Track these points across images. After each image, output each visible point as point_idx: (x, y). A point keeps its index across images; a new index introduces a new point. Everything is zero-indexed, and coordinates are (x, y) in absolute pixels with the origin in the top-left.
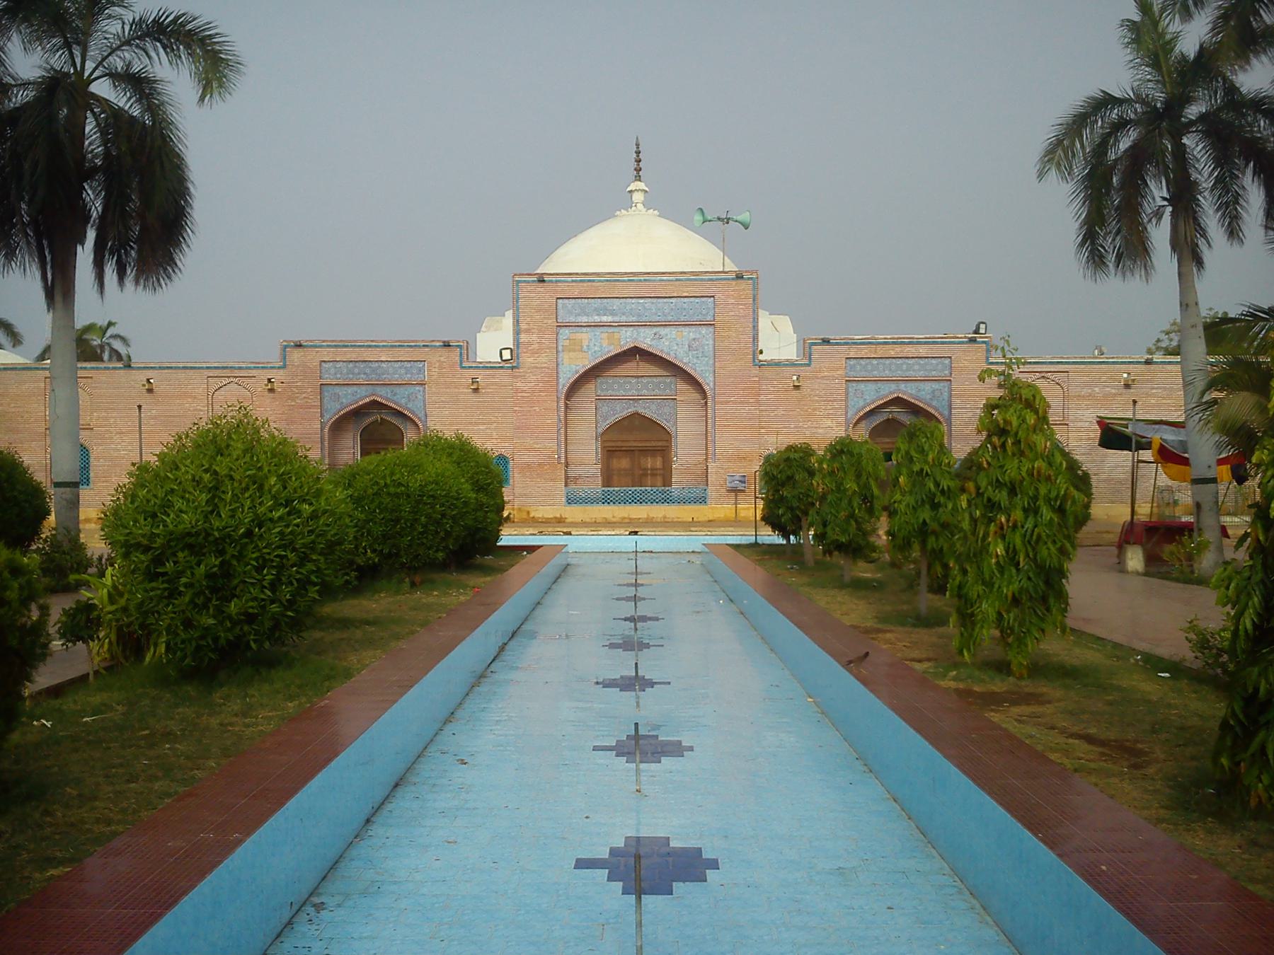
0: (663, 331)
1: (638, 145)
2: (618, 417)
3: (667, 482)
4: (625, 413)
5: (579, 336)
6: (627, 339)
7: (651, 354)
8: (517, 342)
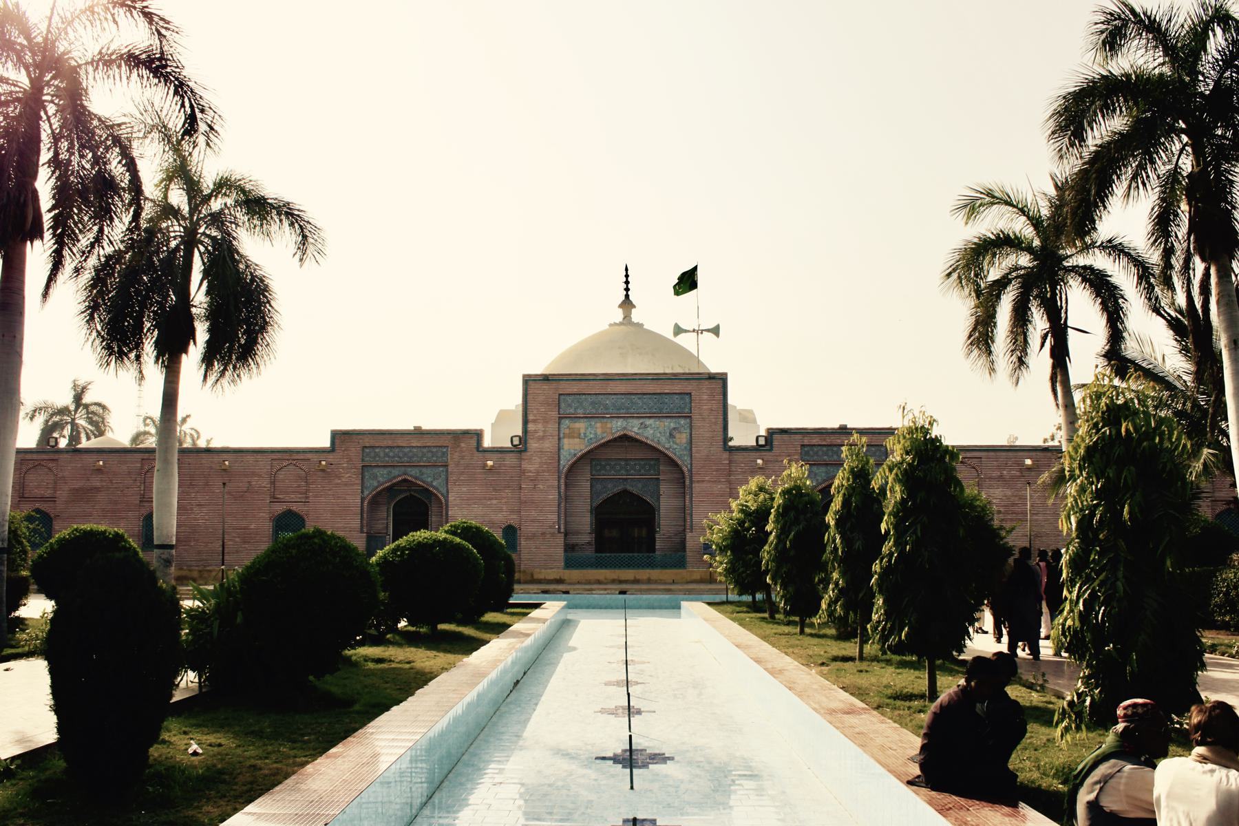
0: (648, 422)
1: (627, 269)
2: (609, 494)
3: (651, 548)
4: (616, 490)
5: (577, 425)
6: (617, 427)
7: (637, 441)
8: (525, 431)
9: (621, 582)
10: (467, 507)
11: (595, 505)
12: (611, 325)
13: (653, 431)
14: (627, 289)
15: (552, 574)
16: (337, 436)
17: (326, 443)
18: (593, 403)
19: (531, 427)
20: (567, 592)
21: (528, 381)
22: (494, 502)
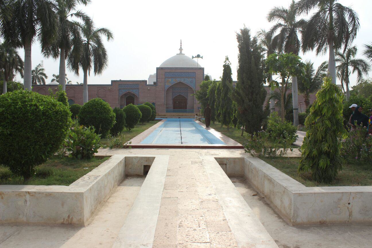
0: (185, 79)
1: (181, 40)
3: (186, 108)
4: (178, 95)
5: (169, 80)
6: (178, 80)
9: (179, 116)
10: (144, 99)
12: (177, 54)
13: (187, 81)
14: (181, 45)
15: (163, 114)
16: (112, 81)
17: (110, 83)
18: (173, 74)
19: (158, 80)
20: (167, 118)
21: (158, 69)
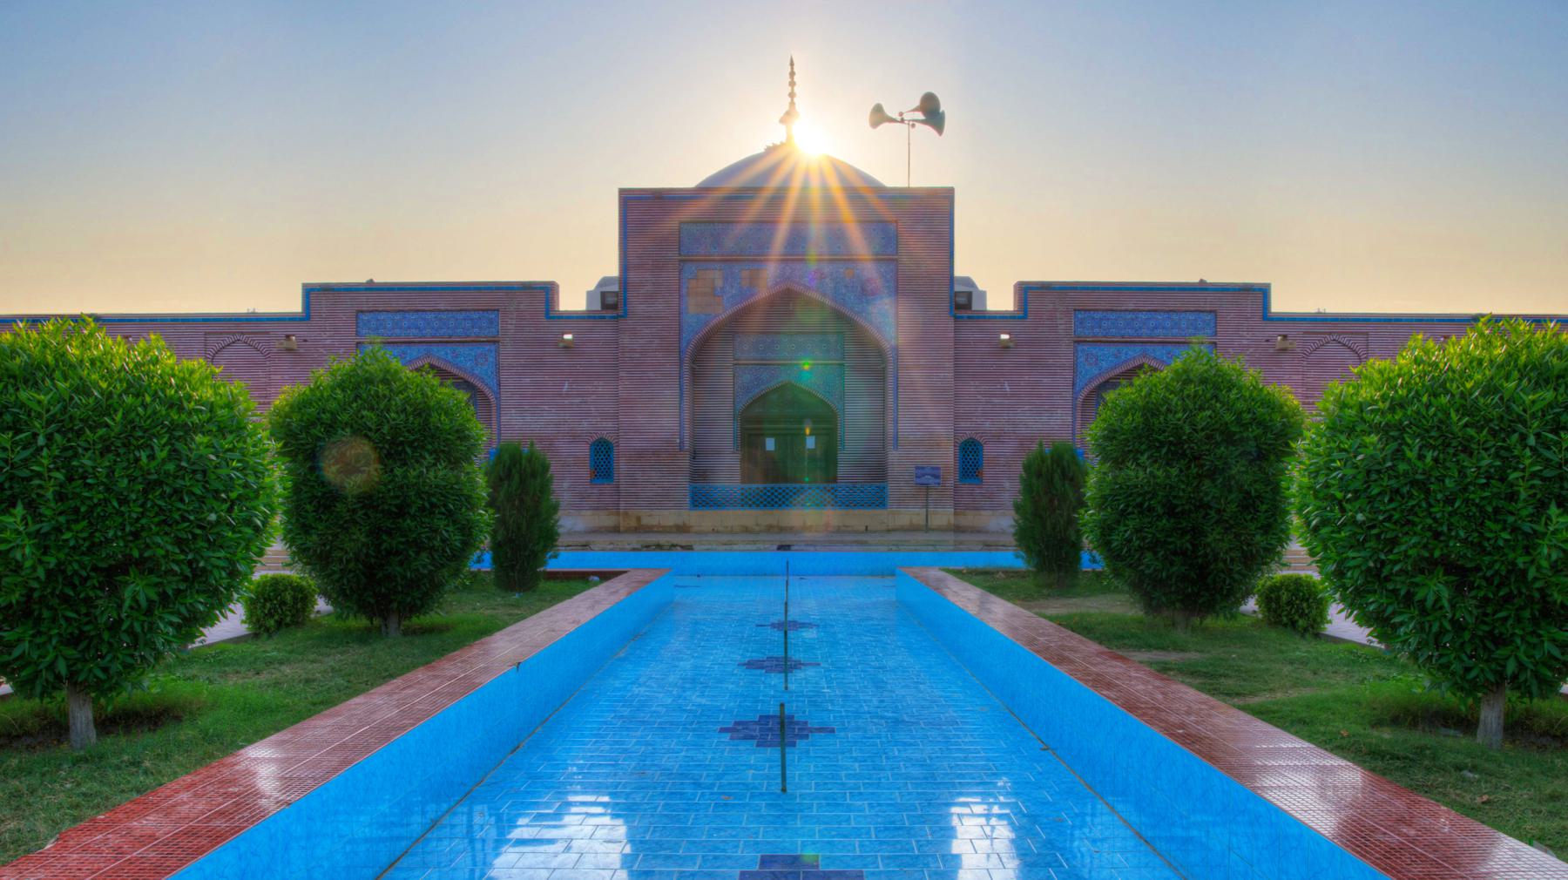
1: (792, 64)
11: (740, 407)
15: (669, 517)
16: (312, 293)
17: (295, 305)
22: (577, 400)
